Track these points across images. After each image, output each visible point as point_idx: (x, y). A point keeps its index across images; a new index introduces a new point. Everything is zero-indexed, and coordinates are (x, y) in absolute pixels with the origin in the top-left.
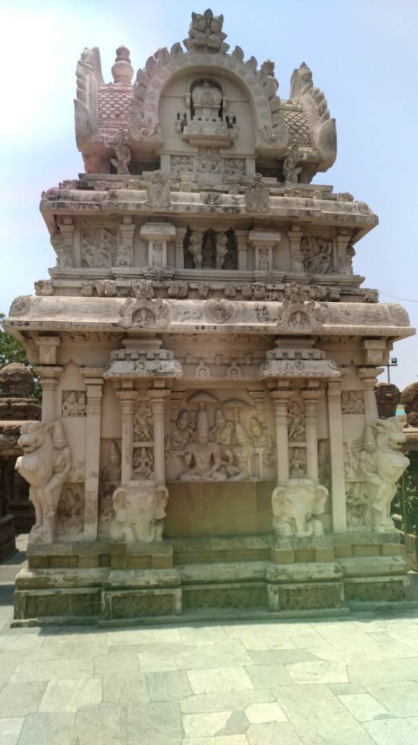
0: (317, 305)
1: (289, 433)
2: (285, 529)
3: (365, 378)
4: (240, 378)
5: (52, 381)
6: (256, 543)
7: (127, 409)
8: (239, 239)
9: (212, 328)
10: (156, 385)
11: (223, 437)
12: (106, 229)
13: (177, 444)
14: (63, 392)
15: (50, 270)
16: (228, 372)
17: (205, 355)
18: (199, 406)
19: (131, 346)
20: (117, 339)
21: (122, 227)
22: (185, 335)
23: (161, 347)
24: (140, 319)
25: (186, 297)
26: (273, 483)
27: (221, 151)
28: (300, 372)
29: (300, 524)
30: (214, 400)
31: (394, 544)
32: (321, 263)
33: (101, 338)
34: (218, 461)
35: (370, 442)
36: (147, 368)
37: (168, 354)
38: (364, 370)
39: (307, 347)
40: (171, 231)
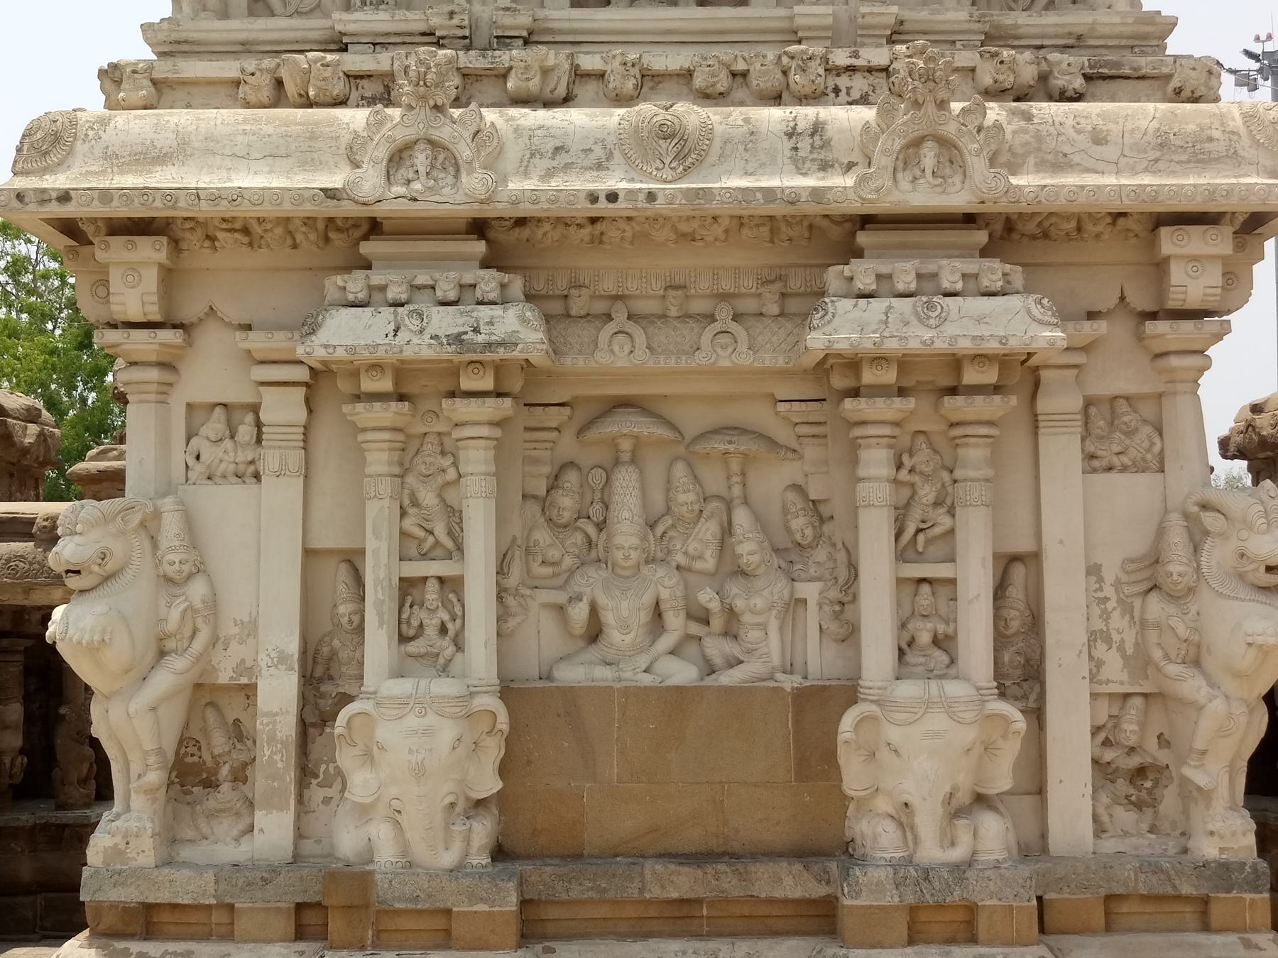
0: (995, 112)
1: (898, 536)
2: (878, 835)
3: (1165, 354)
4: (744, 359)
5: (153, 374)
6: (788, 881)
7: (379, 461)
9: (642, 197)
10: (466, 384)
11: (692, 547)
13: (549, 570)
15: (146, 28)
17: (632, 287)
18: (616, 449)
19: (392, 261)
20: (348, 238)
22: (562, 222)
23: (486, 264)
24: (411, 175)
25: (567, 100)
26: (849, 693)
28: (928, 334)
29: (928, 822)
30: (661, 432)
31: (1248, 896)
33: (299, 238)
34: (675, 622)
35: (1177, 567)
36: (430, 331)
37: (503, 286)
38: (1161, 327)
39: (963, 252)
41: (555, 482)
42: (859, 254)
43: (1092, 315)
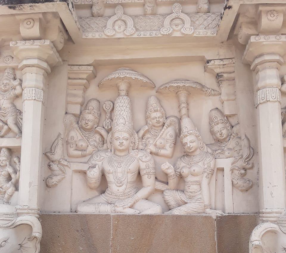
4: (188, 30)
11: (159, 141)
13: (80, 153)
34: (149, 181)
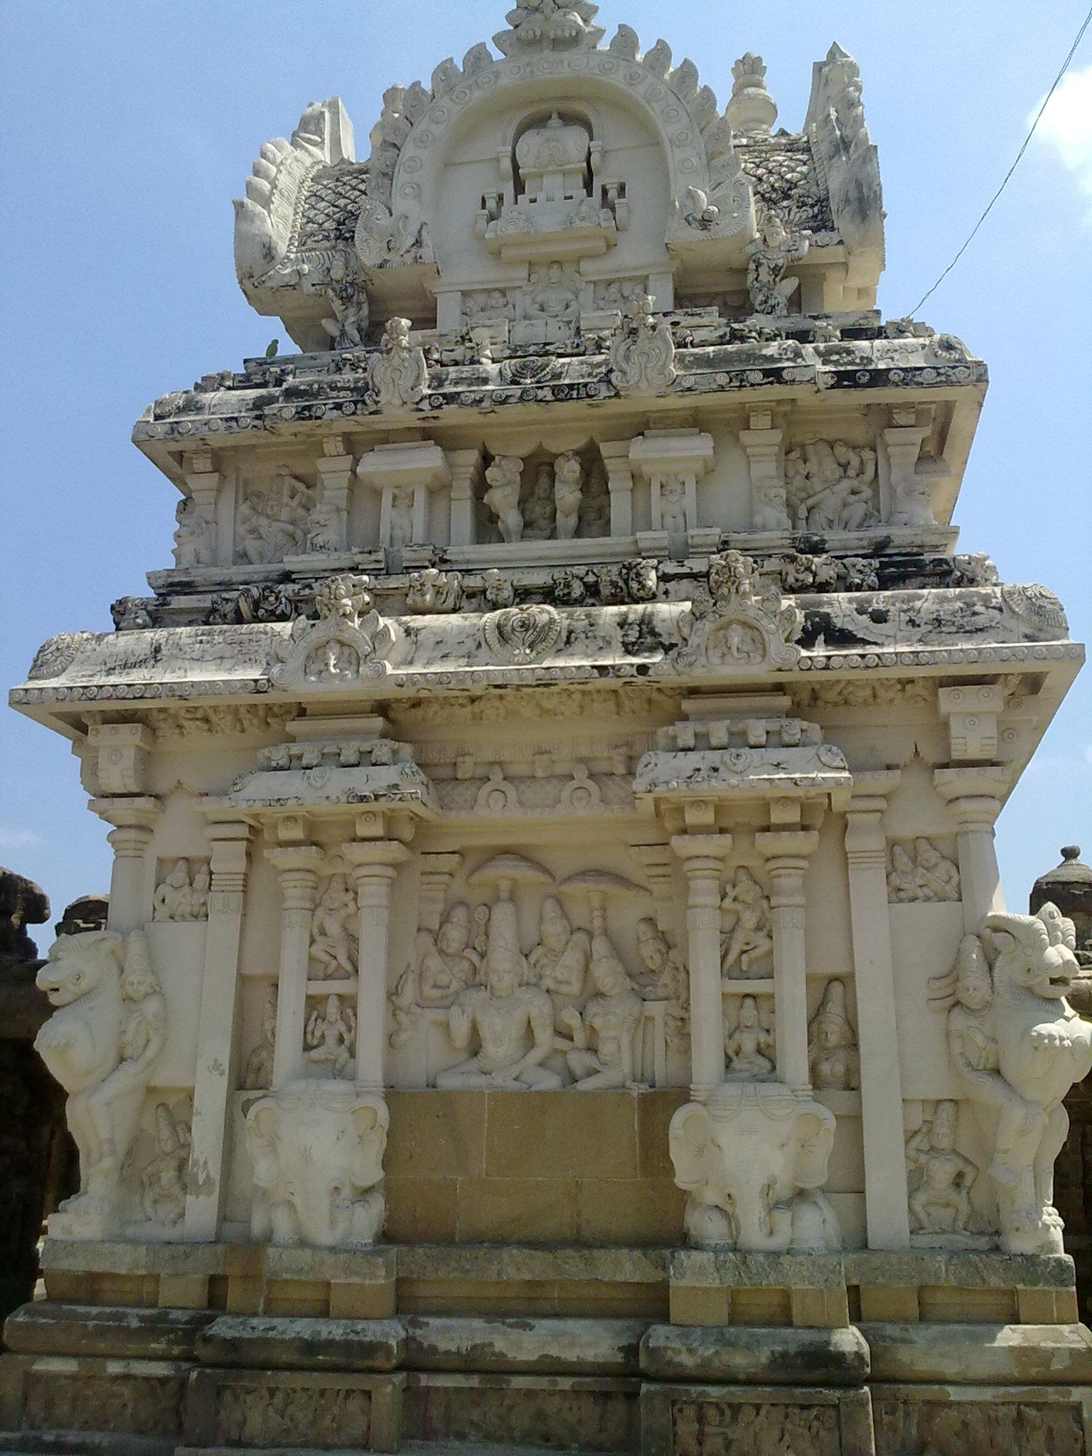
1: (724, 958)
2: (708, 1227)
8: (610, 465)
10: (362, 831)
12: (297, 478)
14: (161, 861)
16: (565, 794)
17: (506, 755)
18: (497, 888)
21: (322, 465)
23: (384, 735)
26: (682, 1095)
27: (586, 266)
32: (845, 505)
33: (246, 724)
34: (544, 1037)
35: (975, 984)
40: (429, 459)
41: (445, 919)
42: (685, 718)
43: (889, 768)
